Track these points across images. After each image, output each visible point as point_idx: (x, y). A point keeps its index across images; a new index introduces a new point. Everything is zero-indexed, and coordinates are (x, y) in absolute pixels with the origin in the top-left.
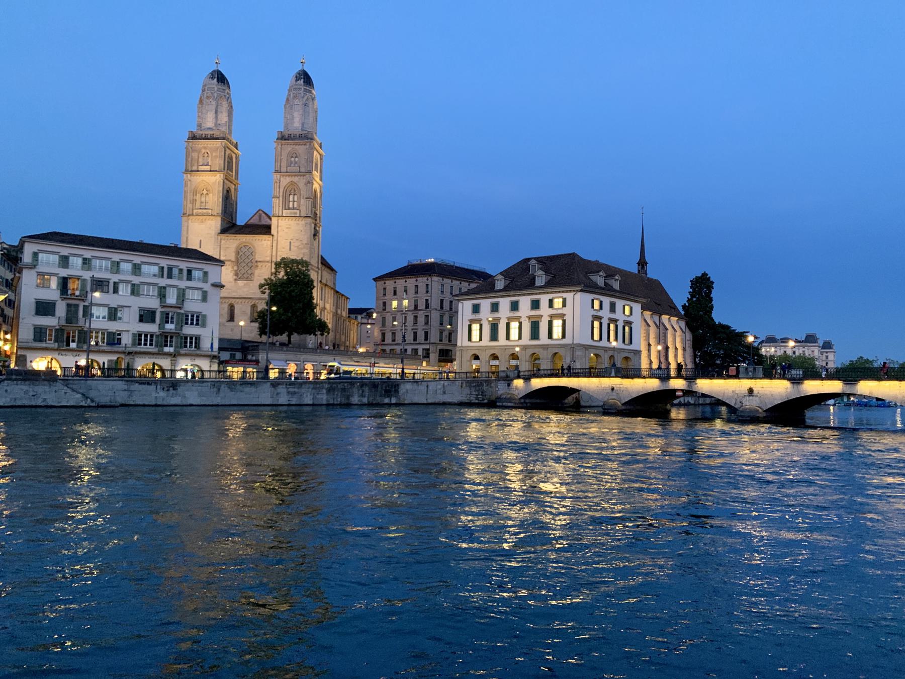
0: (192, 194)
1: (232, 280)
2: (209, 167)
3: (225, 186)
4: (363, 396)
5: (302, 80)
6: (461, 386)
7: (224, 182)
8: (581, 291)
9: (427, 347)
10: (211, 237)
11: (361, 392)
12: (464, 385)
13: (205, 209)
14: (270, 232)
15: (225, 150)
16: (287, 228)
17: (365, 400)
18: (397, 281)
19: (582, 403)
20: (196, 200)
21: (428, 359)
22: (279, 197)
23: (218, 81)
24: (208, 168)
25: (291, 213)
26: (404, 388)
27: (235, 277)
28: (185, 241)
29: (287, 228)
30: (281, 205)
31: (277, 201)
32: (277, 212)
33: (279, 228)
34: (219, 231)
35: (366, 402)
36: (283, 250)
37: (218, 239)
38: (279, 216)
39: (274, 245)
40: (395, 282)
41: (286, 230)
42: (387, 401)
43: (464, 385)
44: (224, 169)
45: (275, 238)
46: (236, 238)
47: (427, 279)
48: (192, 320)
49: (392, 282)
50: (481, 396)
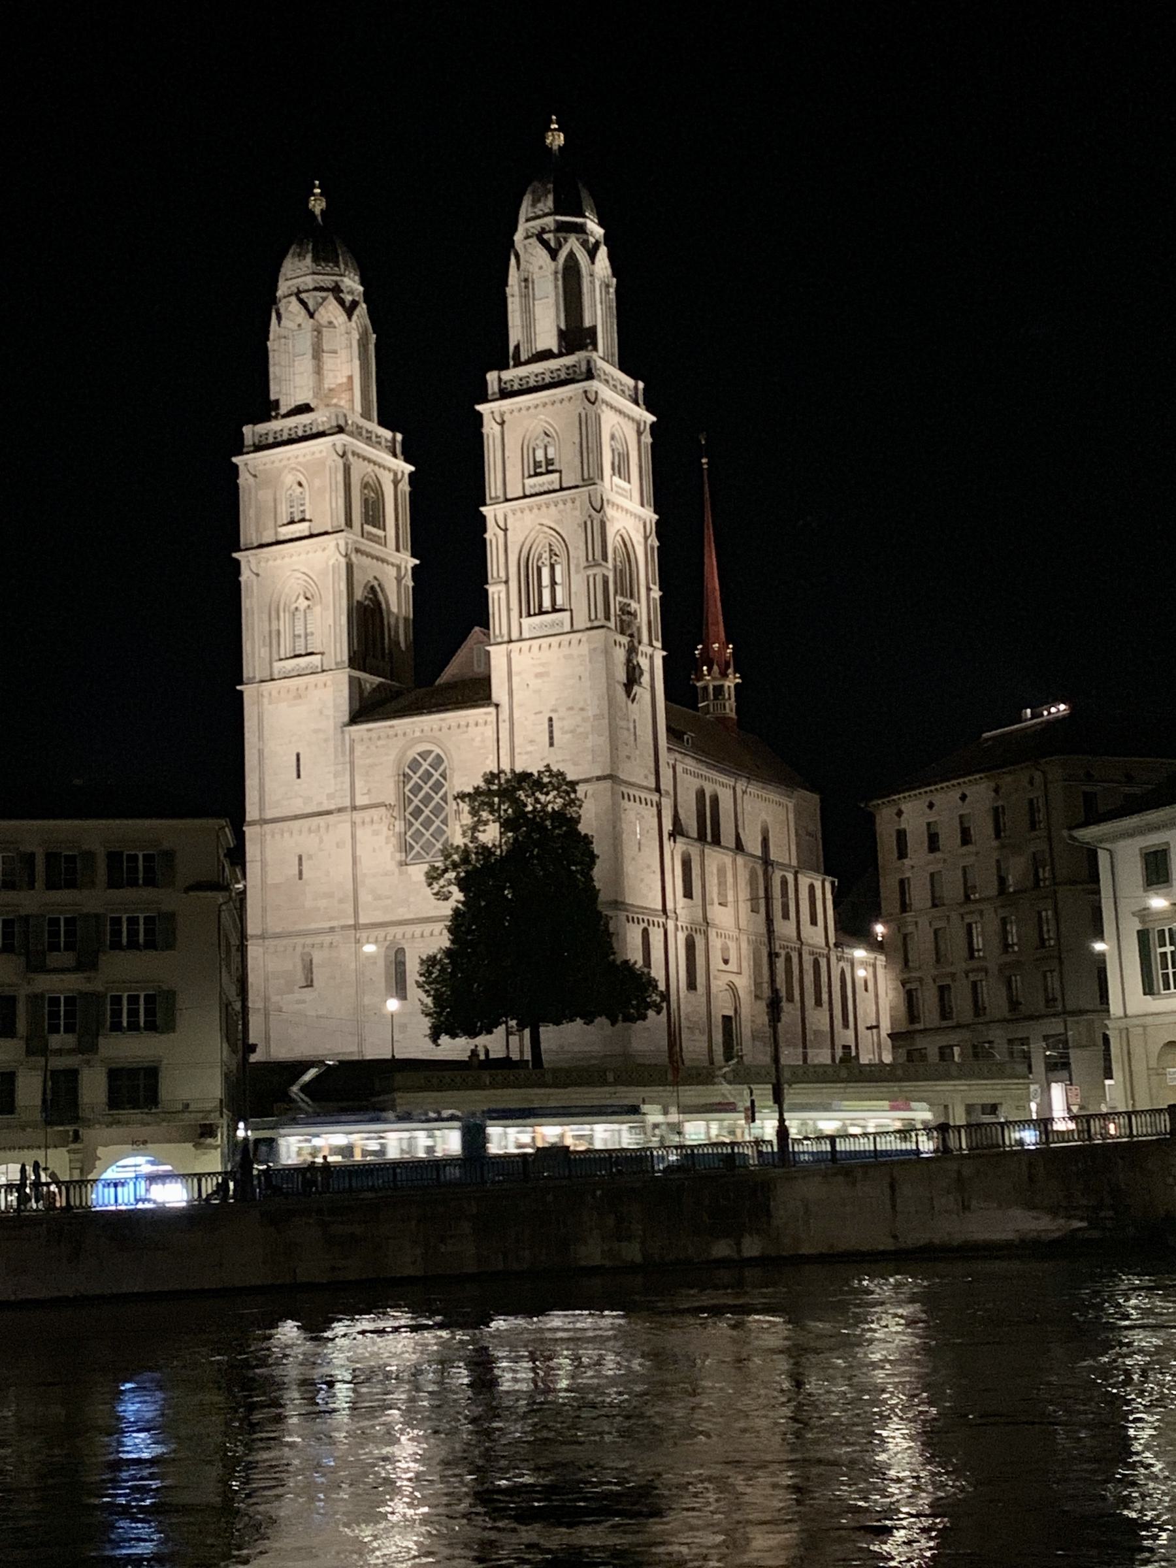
0: (265, 617)
1: (392, 866)
2: (305, 525)
3: (357, 575)
5: (551, 197)
7: (350, 567)
10: (326, 740)
11: (611, 1221)
14: (489, 697)
15: (347, 470)
17: (632, 1252)
18: (938, 799)
20: (279, 632)
21: (1065, 1074)
22: (506, 582)
23: (316, 260)
24: (302, 529)
25: (543, 625)
27: (400, 856)
28: (256, 762)
31: (503, 596)
32: (505, 631)
33: (515, 679)
34: (346, 719)
35: (639, 1258)
36: (530, 748)
37: (343, 739)
38: (510, 641)
40: (931, 806)
41: (535, 683)
42: (722, 1249)
44: (349, 522)
46: (391, 732)
48: (133, 1013)
49: (922, 804)
50: (1111, 1213)
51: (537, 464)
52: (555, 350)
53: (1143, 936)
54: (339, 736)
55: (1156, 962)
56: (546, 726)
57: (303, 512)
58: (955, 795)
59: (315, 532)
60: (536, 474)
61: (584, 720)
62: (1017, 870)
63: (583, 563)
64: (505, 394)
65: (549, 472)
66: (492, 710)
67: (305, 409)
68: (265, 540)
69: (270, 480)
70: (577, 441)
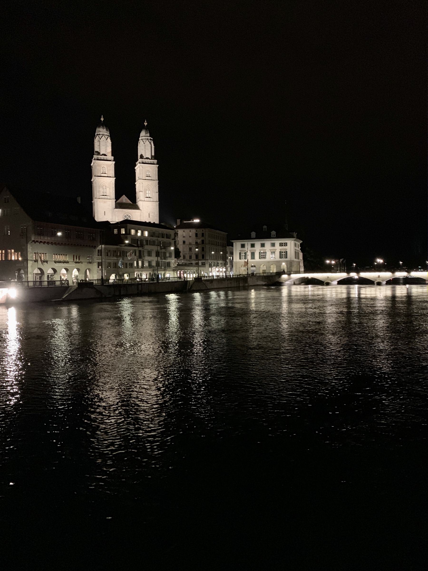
4: (242, 283)
6: (262, 278)
8: (294, 240)
9: (204, 261)
12: (263, 278)
13: (106, 196)
16: (147, 207)
19: (295, 283)
26: (249, 279)
29: (147, 207)
30: (144, 195)
31: (142, 194)
33: (144, 207)
34: (115, 207)
37: (114, 211)
39: (142, 215)
43: (263, 278)
45: (142, 212)
46: (122, 211)
47: (203, 231)
51: (147, 175)
52: (150, 158)
53: (240, 254)
54: (113, 210)
55: (241, 256)
56: (148, 214)
57: (105, 172)
58: (189, 230)
59: (108, 176)
60: (147, 177)
61: (155, 214)
62: (199, 241)
63: (155, 192)
64: (143, 163)
65: (149, 177)
66: (140, 211)
67: (105, 155)
68: (98, 175)
69: (99, 165)
70: (155, 173)
